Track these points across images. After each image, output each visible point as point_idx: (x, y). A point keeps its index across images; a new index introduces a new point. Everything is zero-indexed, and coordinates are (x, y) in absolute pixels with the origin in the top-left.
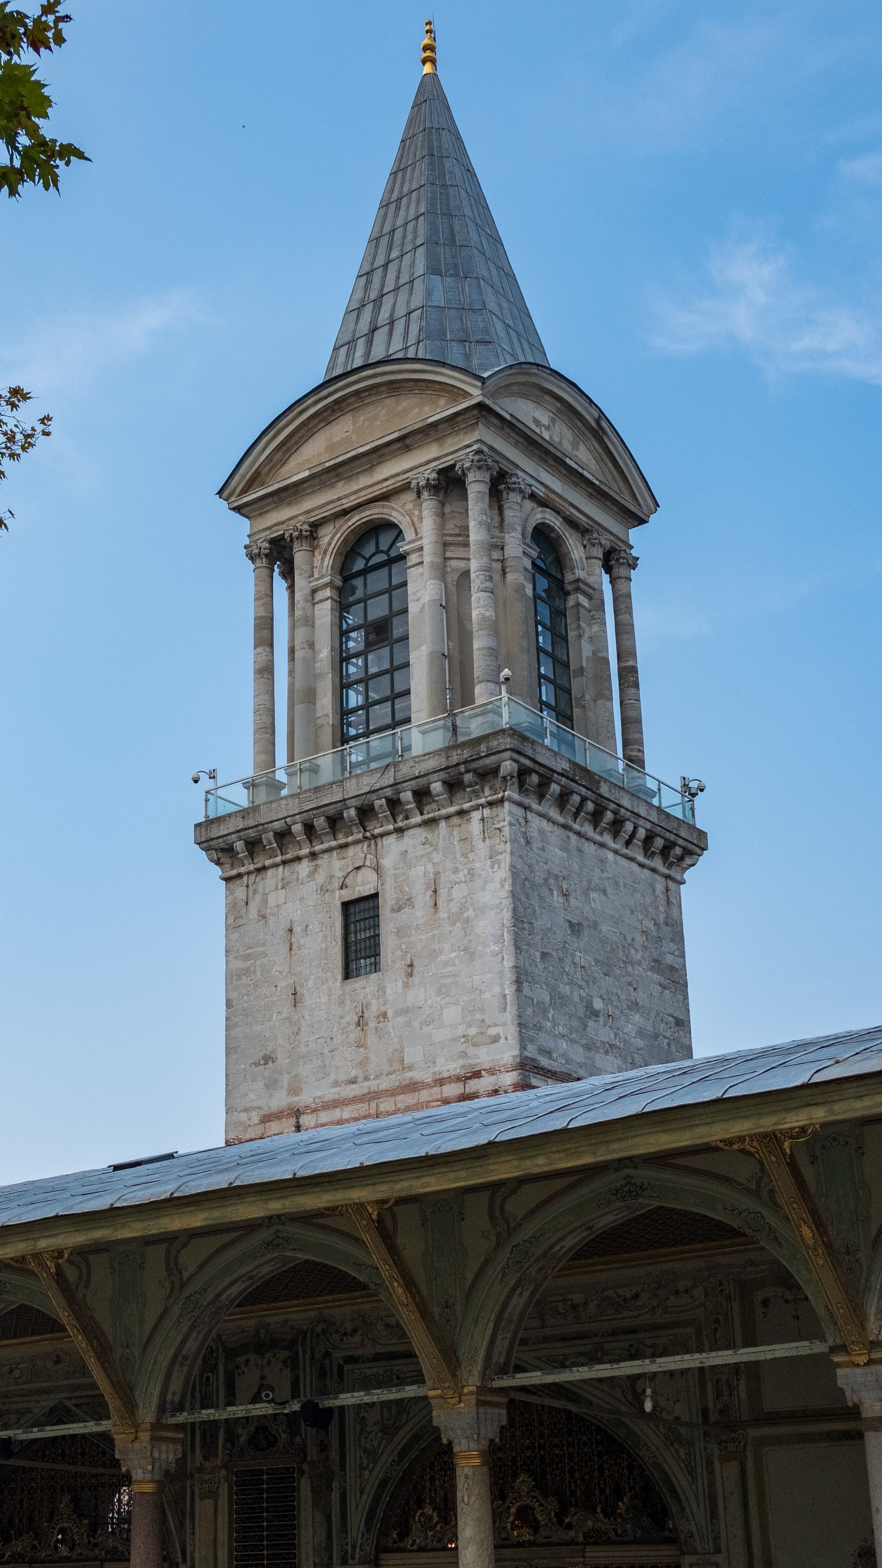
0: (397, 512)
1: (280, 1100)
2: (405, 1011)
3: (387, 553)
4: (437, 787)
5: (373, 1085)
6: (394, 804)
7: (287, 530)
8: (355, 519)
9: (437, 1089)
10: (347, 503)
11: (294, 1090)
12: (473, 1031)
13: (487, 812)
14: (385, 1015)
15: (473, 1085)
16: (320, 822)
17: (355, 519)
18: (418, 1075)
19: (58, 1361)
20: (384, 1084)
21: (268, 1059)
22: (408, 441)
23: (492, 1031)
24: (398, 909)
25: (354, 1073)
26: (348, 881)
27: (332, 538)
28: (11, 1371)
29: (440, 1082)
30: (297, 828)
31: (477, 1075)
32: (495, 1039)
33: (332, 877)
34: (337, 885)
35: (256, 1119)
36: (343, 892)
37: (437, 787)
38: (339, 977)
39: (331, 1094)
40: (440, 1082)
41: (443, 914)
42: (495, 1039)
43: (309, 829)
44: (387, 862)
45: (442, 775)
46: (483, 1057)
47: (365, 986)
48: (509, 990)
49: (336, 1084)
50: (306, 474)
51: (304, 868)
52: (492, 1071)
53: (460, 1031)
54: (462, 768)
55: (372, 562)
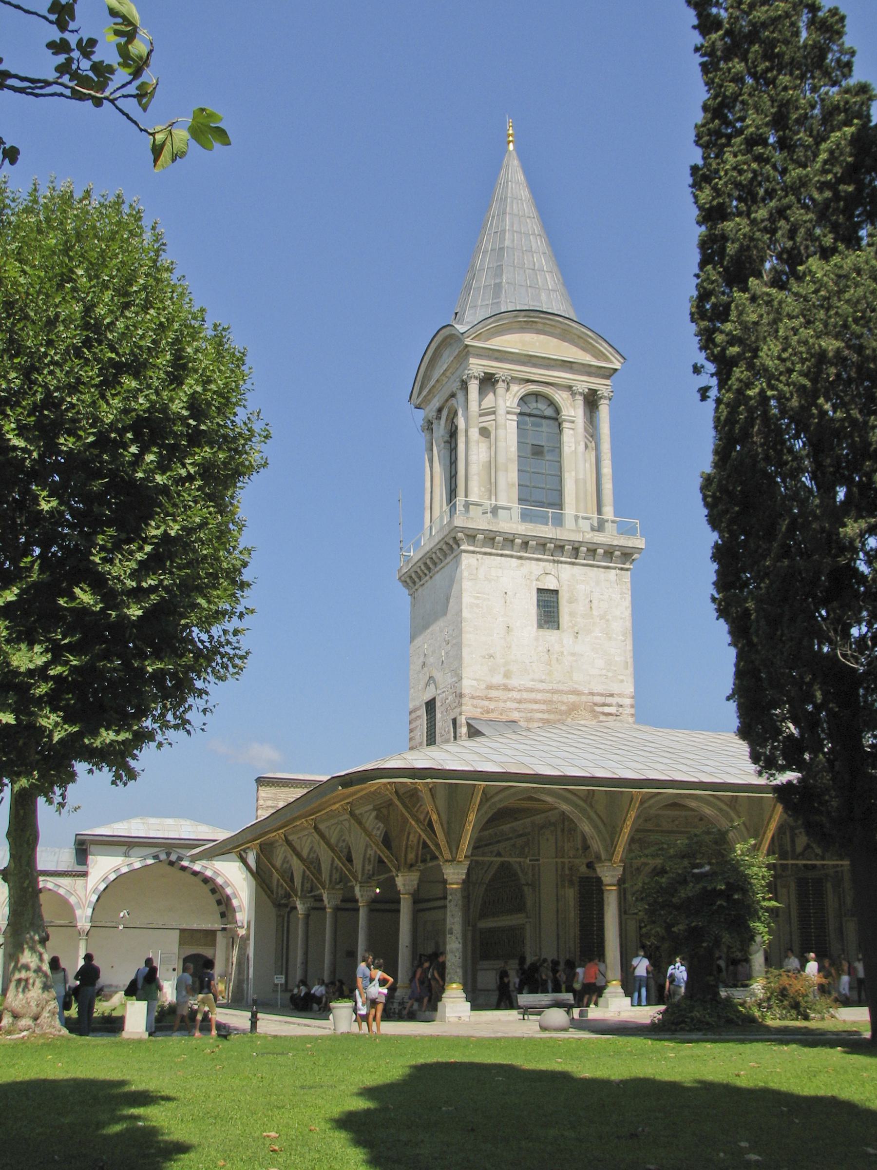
0: (561, 397)
1: (498, 679)
2: (573, 654)
4: (600, 551)
5: (555, 686)
6: (576, 550)
7: (500, 374)
8: (533, 388)
9: (590, 697)
11: (507, 675)
12: (610, 674)
13: (618, 571)
14: (562, 653)
15: (609, 700)
16: (532, 543)
17: (533, 388)
18: (581, 688)
19: (701, 820)
20: (561, 687)
21: (491, 656)
22: (574, 365)
23: (621, 677)
24: (570, 602)
25: (543, 677)
26: (541, 578)
27: (517, 390)
28: (673, 821)
29: (593, 694)
30: (518, 541)
31: (612, 695)
32: (622, 681)
34: (534, 578)
35: (483, 686)
37: (600, 551)
38: (536, 626)
39: (530, 684)
40: (593, 694)
41: (595, 613)
42: (622, 681)
43: (525, 545)
45: (606, 548)
46: (615, 688)
47: (550, 636)
48: (630, 661)
49: (533, 680)
50: (517, 351)
52: (620, 695)
53: (604, 672)
54: (617, 548)
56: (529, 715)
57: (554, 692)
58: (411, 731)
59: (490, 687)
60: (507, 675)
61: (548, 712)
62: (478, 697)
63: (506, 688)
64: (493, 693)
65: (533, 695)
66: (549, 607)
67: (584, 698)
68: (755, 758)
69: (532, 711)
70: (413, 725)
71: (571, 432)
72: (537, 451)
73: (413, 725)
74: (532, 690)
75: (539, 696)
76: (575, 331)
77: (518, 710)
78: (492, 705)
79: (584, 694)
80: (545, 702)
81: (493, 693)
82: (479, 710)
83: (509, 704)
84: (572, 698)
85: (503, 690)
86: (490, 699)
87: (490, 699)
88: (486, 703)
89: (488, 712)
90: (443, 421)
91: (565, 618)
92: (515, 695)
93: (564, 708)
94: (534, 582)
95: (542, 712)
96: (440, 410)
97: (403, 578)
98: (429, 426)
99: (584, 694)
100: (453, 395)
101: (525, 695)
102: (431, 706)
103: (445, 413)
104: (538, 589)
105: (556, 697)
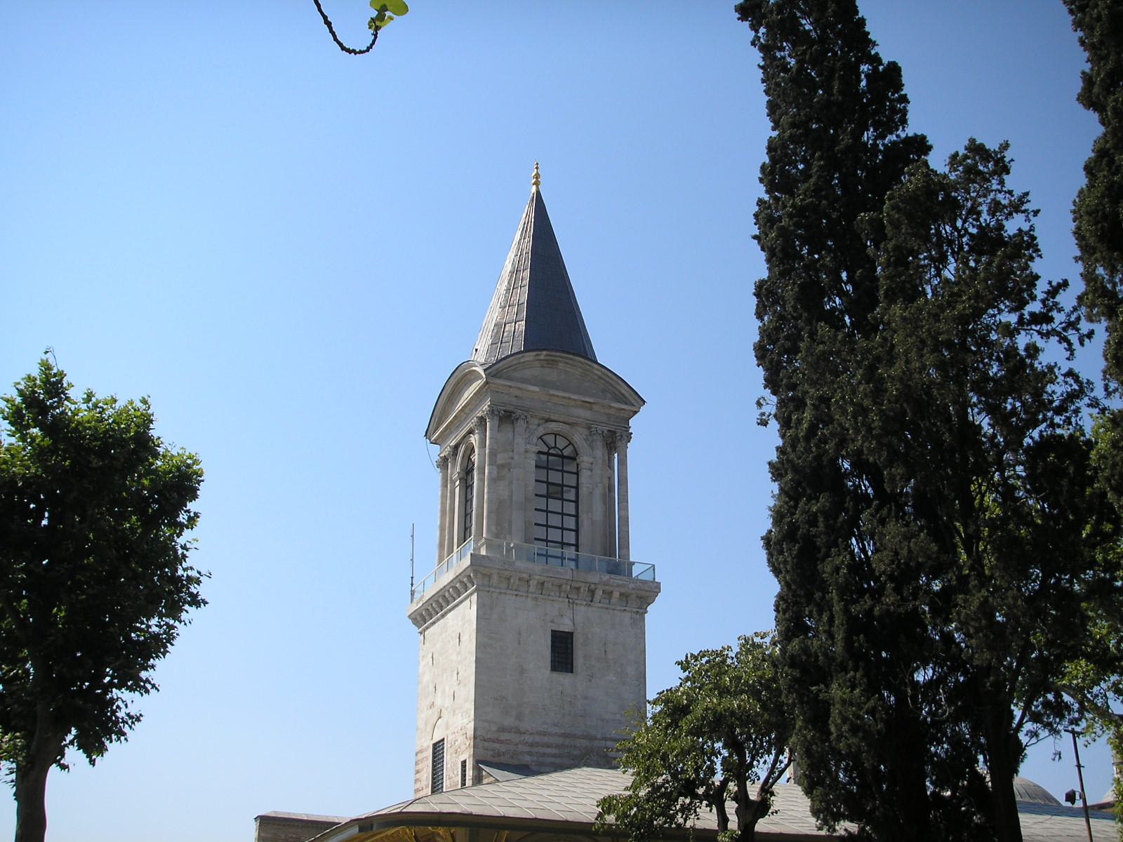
0: (578, 437)
1: (509, 721)
2: (586, 698)
3: (561, 451)
4: (616, 594)
9: (603, 742)
10: (552, 418)
14: (575, 696)
22: (594, 406)
29: (606, 739)
33: (546, 614)
36: (553, 625)
37: (616, 594)
40: (606, 739)
44: (579, 619)
47: (564, 679)
51: (530, 603)
53: (618, 717)
55: (551, 451)
56: (541, 759)
57: (565, 735)
58: (417, 772)
59: (502, 729)
60: (519, 717)
61: (560, 756)
62: (489, 740)
63: (519, 732)
64: (505, 736)
65: (546, 739)
66: (563, 651)
67: (596, 743)
68: (815, 812)
69: (544, 755)
70: (420, 767)
71: (589, 473)
72: (554, 491)
73: (420, 767)
74: (544, 734)
75: (551, 740)
76: (596, 372)
77: (530, 754)
78: (503, 748)
79: (596, 739)
80: (557, 746)
81: (505, 736)
82: (490, 753)
83: (521, 748)
84: (584, 743)
85: (515, 732)
86: (501, 742)
87: (501, 742)
88: (497, 746)
89: (499, 755)
90: (459, 459)
91: (579, 660)
92: (528, 738)
93: (576, 752)
94: (549, 624)
95: (554, 756)
96: (456, 447)
97: (413, 616)
98: (443, 463)
99: (596, 739)
100: (471, 432)
101: (538, 739)
102: (438, 748)
103: (462, 449)
104: (552, 631)
105: (567, 742)
